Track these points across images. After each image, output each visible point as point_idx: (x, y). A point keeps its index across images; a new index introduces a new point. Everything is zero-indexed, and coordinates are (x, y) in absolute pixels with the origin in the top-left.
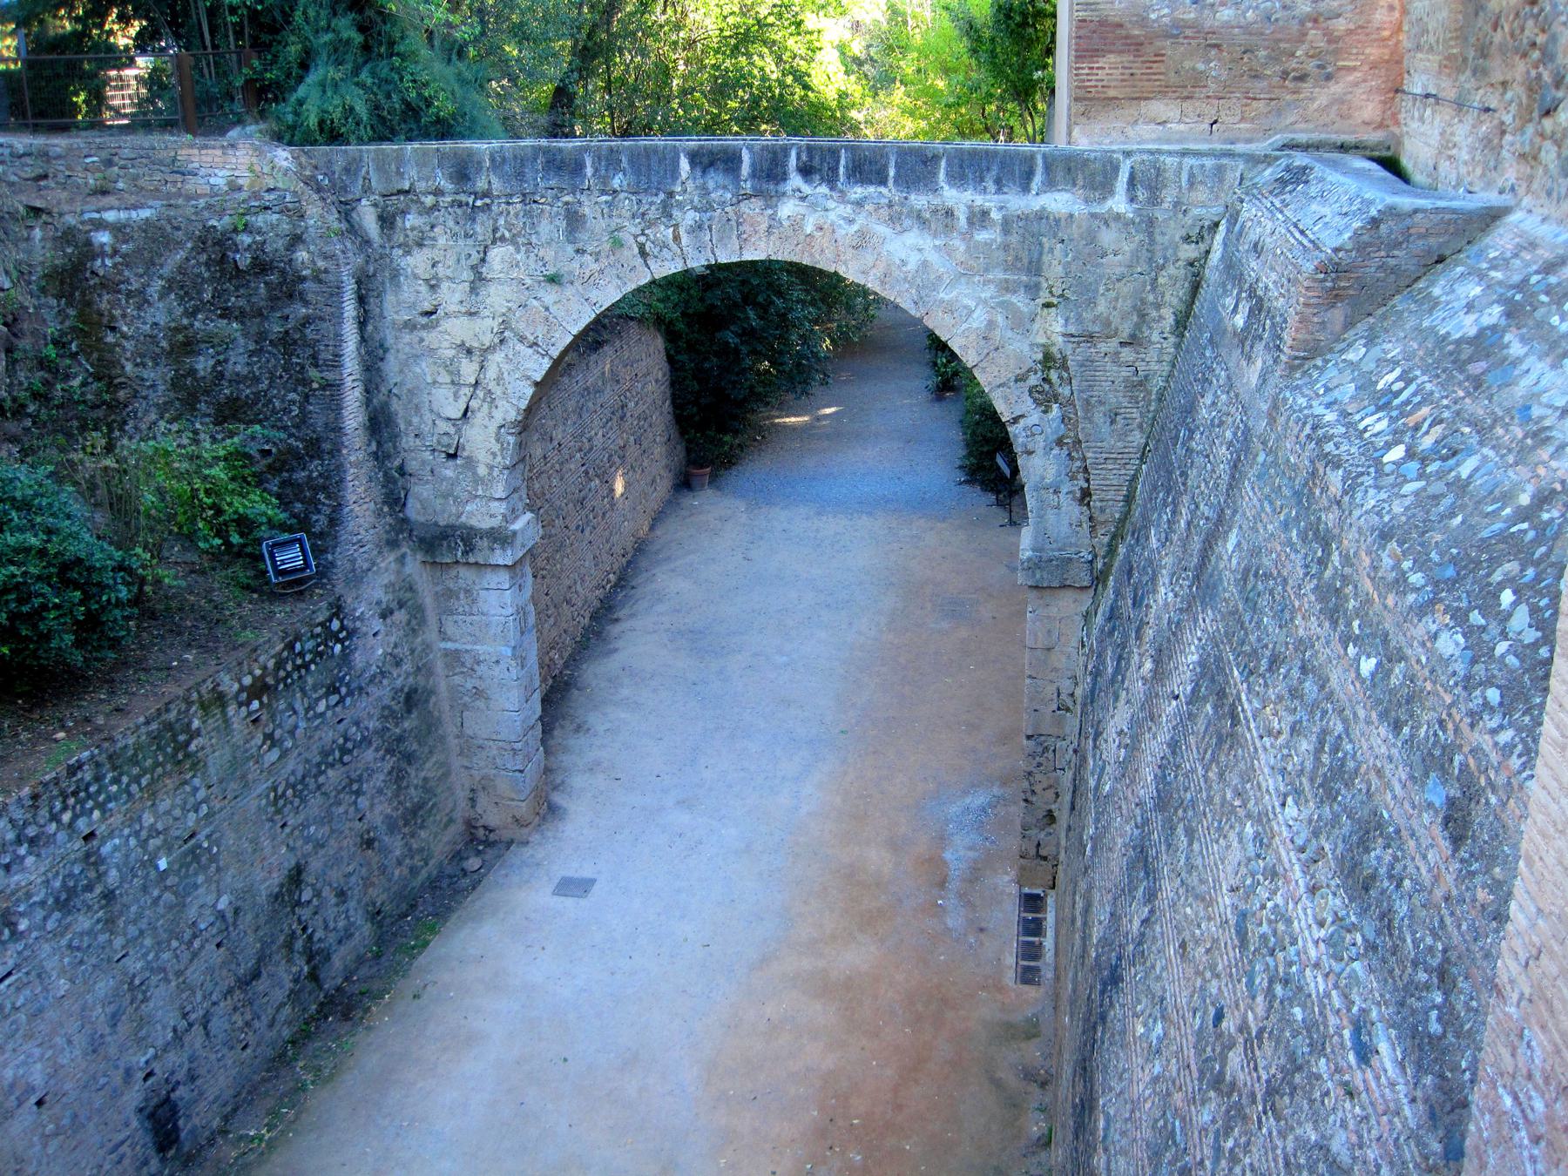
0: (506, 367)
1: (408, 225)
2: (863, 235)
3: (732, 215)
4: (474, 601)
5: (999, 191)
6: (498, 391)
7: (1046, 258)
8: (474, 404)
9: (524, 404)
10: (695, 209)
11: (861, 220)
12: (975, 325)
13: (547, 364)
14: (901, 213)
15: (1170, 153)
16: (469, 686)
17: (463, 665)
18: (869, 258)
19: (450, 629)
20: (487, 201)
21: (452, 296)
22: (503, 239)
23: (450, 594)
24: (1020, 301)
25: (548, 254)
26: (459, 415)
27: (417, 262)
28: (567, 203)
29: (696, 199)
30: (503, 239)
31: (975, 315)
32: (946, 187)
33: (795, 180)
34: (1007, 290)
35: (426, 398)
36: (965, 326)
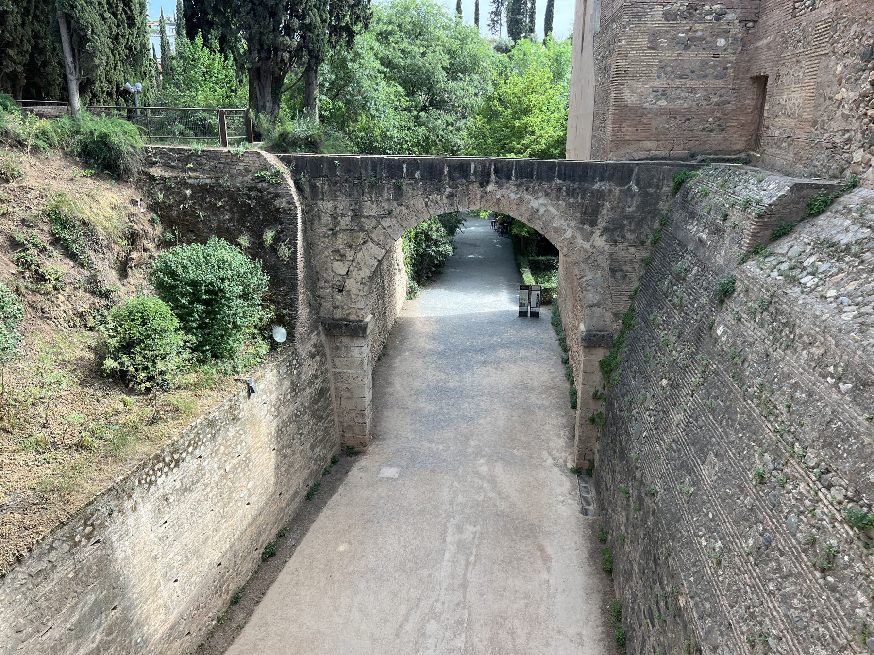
2: (521, 199)
8: (351, 268)
10: (449, 187)
11: (520, 192)
16: (344, 387)
17: (342, 378)
18: (523, 209)
19: (337, 363)
21: (344, 222)
23: (338, 348)
24: (587, 227)
28: (394, 184)
33: (493, 176)
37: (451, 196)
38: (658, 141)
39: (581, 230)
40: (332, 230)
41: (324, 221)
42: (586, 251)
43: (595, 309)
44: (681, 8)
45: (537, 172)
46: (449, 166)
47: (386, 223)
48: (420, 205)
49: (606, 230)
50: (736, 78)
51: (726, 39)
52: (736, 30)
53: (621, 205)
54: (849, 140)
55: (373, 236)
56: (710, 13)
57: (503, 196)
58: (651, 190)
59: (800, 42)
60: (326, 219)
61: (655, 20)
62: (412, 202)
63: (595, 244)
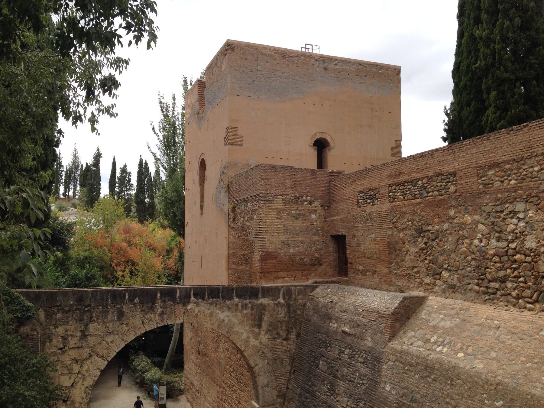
0: (90, 365)
1: (58, 317)
2: (212, 313)
3: (173, 309)
5: (250, 299)
9: (96, 378)
10: (161, 308)
12: (244, 338)
13: (106, 363)
15: (293, 286)
18: (214, 320)
21: (73, 342)
22: (94, 321)
24: (256, 330)
25: (110, 325)
26: (71, 385)
27: (61, 330)
29: (162, 305)
30: (94, 321)
31: (244, 335)
32: (235, 297)
33: (193, 298)
35: (57, 380)
36: (241, 339)
37: (162, 313)
38: (288, 272)
39: (252, 331)
40: (61, 349)
41: (54, 342)
42: (256, 347)
44: (291, 198)
45: (222, 294)
46: (161, 293)
47: (109, 339)
48: (138, 323)
49: (268, 331)
50: (323, 236)
51: (316, 215)
52: (320, 210)
53: (275, 312)
54: (418, 272)
55: (98, 350)
56: (305, 201)
57: (200, 312)
58: (291, 303)
59: (368, 220)
60: (57, 342)
61: (278, 204)
62: (131, 321)
63: (262, 341)
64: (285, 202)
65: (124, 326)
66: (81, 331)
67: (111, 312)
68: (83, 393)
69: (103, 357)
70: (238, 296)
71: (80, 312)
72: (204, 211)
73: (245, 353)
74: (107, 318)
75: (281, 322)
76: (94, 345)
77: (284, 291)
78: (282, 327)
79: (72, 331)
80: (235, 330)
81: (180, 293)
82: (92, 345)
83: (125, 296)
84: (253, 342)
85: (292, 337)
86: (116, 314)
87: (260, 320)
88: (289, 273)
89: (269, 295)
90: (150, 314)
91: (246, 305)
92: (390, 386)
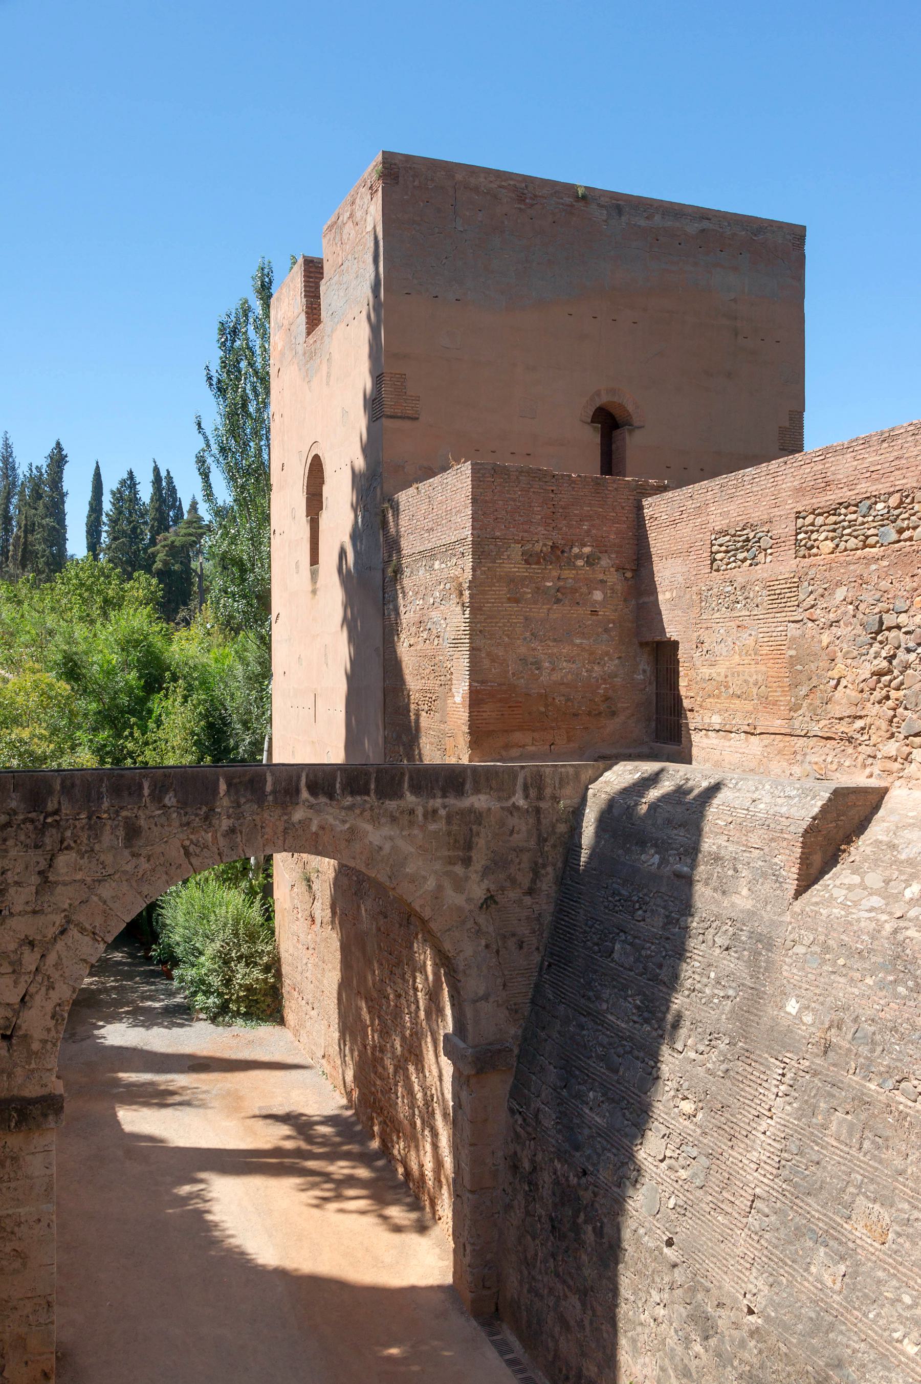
2: (352, 830)
4: (20, 1168)
6: (56, 975)
7: (475, 840)
8: (32, 990)
14: (379, 814)
17: (4, 1229)
20: (57, 818)
24: (459, 869)
32: (408, 794)
33: (305, 794)
34: (450, 863)
37: (232, 831)
38: (533, 731)
42: (460, 909)
43: (482, 1005)
44: (544, 549)
45: (377, 787)
49: (486, 872)
57: (322, 828)
64: (529, 558)
65: (142, 860)
66: (39, 873)
67: (108, 828)
68: (48, 1017)
69: (94, 933)
70: (416, 789)
71: (36, 828)
72: (318, 585)
73: (433, 925)
74: (100, 842)
75: (519, 850)
76: (70, 905)
77: (525, 779)
78: (519, 864)
79: (18, 874)
80: (407, 870)
81: (274, 784)
82: (66, 906)
83: (141, 787)
84: (453, 898)
85: (544, 887)
86: (121, 833)
87: (469, 846)
88: (536, 735)
89: (491, 789)
90: (203, 833)
91: (435, 811)
92: (798, 1002)
